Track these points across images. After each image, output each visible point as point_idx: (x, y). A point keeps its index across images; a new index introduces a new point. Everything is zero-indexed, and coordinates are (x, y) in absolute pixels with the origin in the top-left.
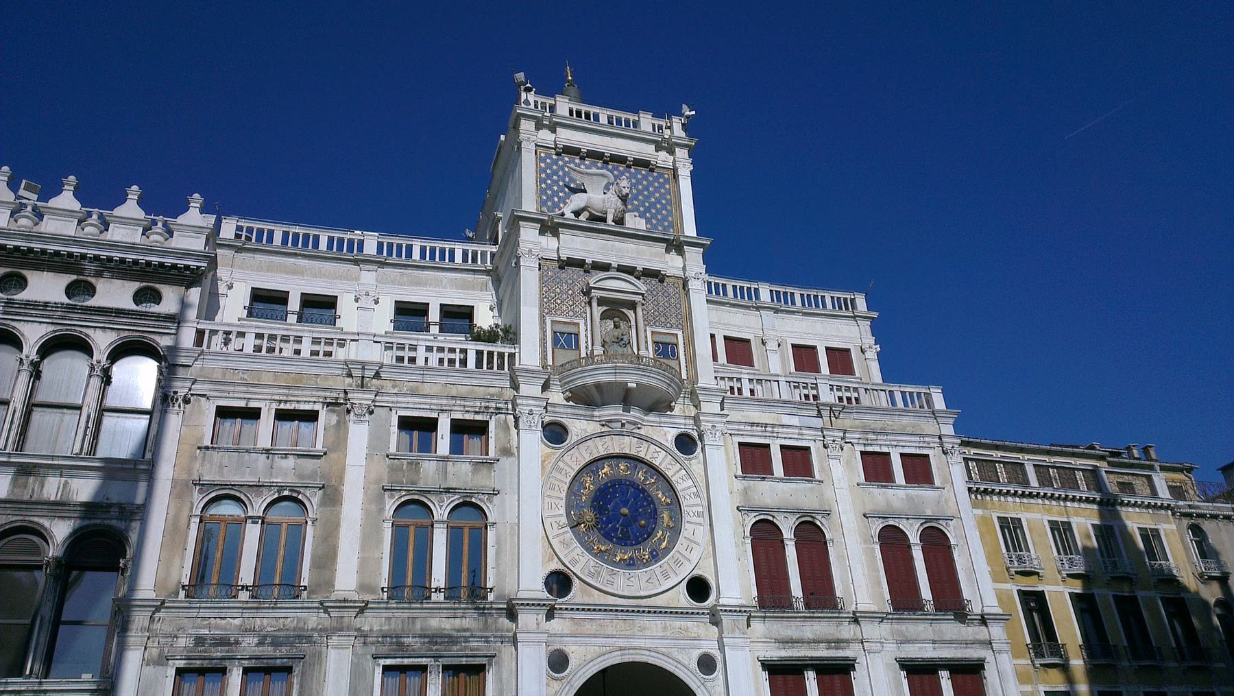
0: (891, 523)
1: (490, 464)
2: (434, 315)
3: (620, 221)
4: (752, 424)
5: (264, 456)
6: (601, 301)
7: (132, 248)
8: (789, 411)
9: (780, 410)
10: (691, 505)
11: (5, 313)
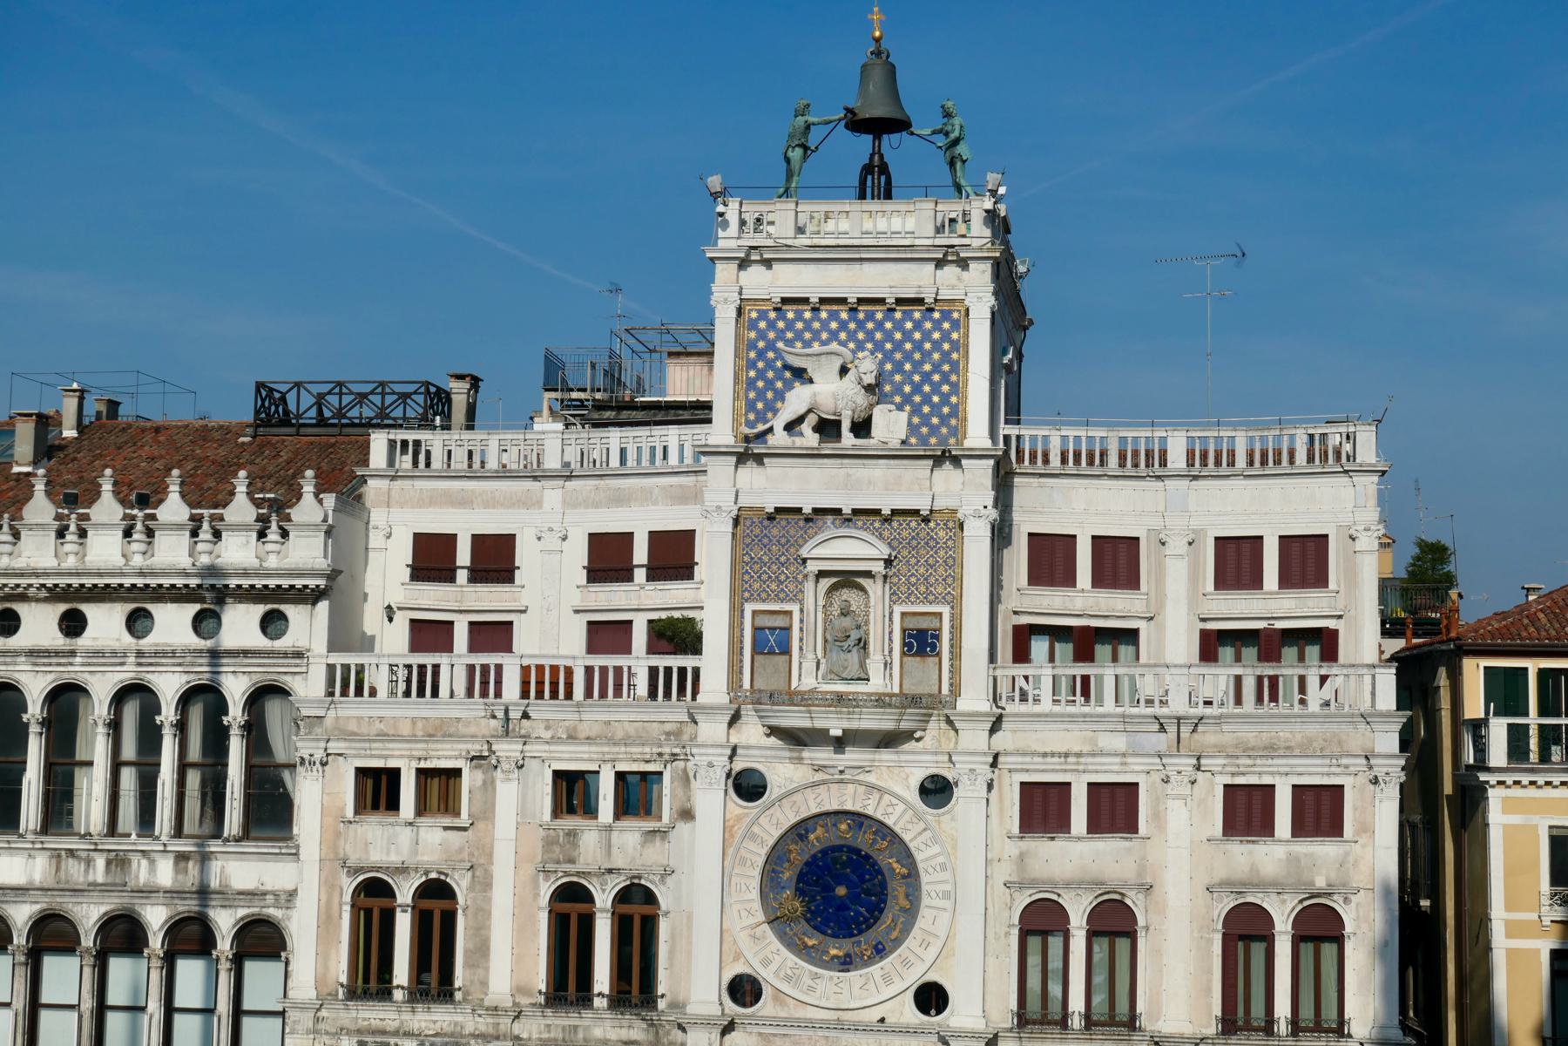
0: (1250, 899)
1: (662, 834)
2: (640, 554)
3: (862, 427)
4: (1045, 755)
5: (409, 828)
6: (822, 574)
7: (245, 573)
8: (1111, 727)
9: (1095, 727)
10: (931, 882)
11: (140, 664)
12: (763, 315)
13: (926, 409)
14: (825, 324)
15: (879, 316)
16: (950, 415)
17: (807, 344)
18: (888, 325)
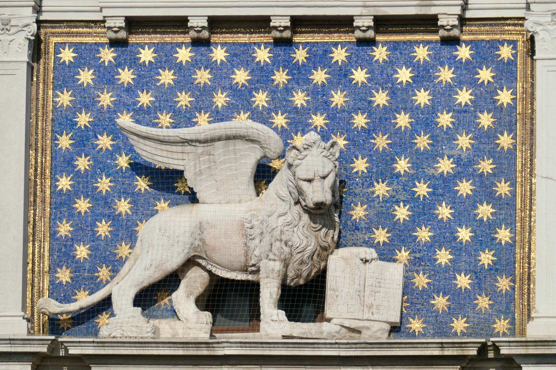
3: (305, 297)
12: (86, 55)
13: (443, 257)
14: (222, 74)
15: (340, 55)
16: (495, 269)
17: (184, 118)
18: (360, 76)
